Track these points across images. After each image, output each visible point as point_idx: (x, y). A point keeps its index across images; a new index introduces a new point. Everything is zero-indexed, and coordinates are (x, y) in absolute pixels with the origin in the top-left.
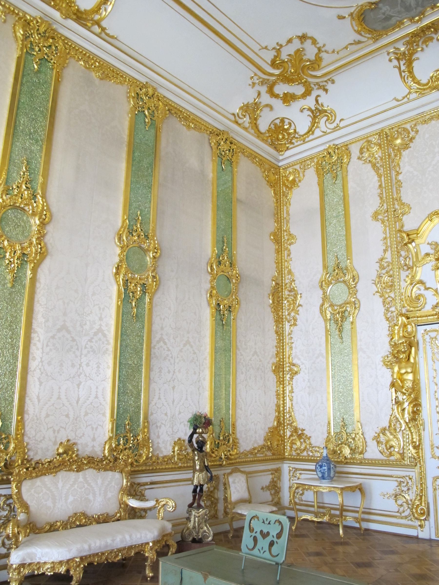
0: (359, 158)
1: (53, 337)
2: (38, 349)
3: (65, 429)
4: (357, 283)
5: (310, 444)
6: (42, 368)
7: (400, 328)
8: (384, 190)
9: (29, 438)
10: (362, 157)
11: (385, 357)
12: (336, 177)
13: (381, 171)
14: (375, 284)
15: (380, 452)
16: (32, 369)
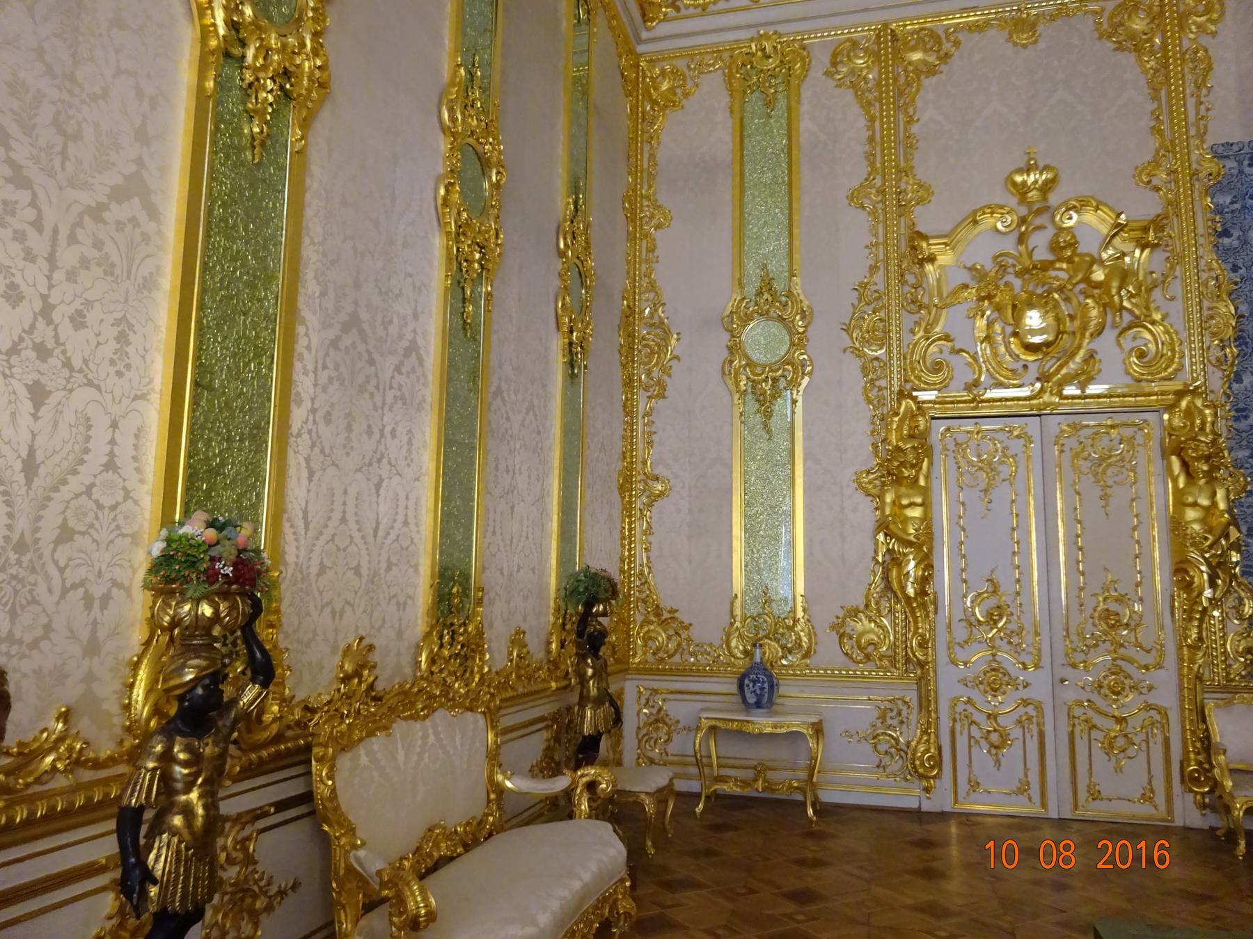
0: (827, 73)
1: (334, 344)
2: (306, 373)
3: (352, 606)
4: (809, 323)
5: (689, 640)
6: (314, 430)
7: (902, 421)
8: (878, 149)
9: (287, 636)
10: (838, 72)
11: (862, 473)
12: (769, 103)
13: (875, 111)
14: (847, 331)
15: (847, 654)
16: (294, 430)
